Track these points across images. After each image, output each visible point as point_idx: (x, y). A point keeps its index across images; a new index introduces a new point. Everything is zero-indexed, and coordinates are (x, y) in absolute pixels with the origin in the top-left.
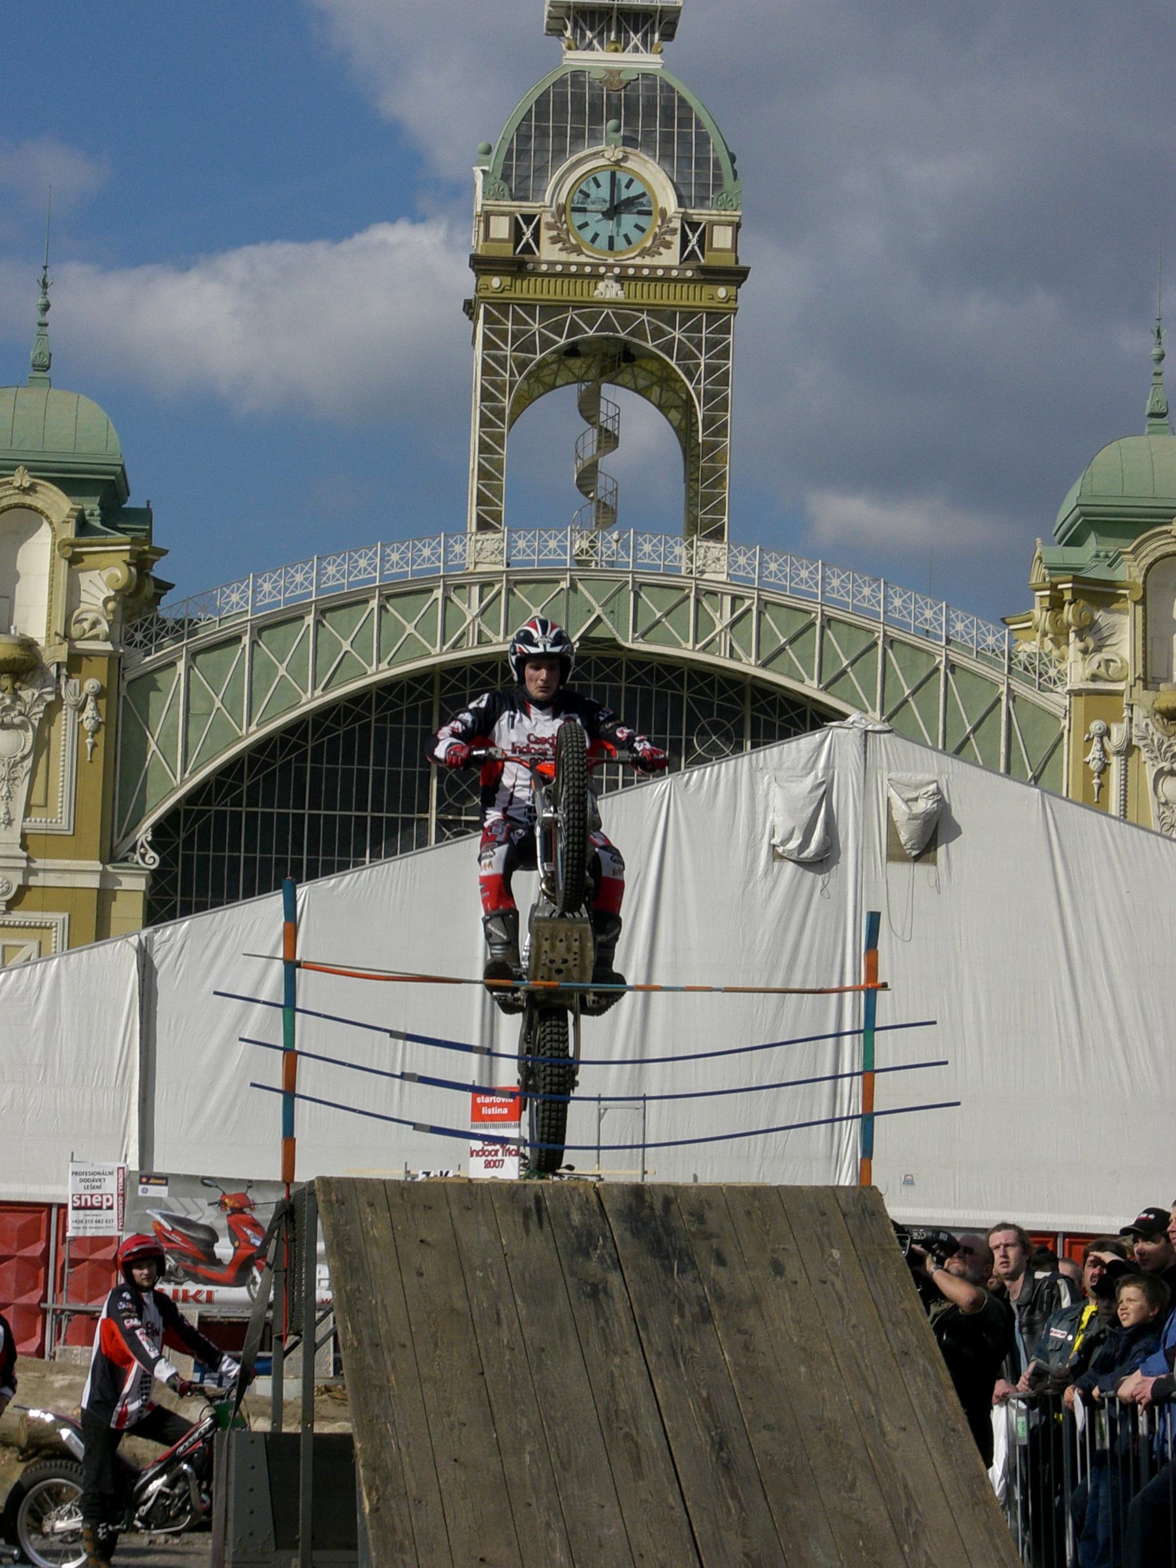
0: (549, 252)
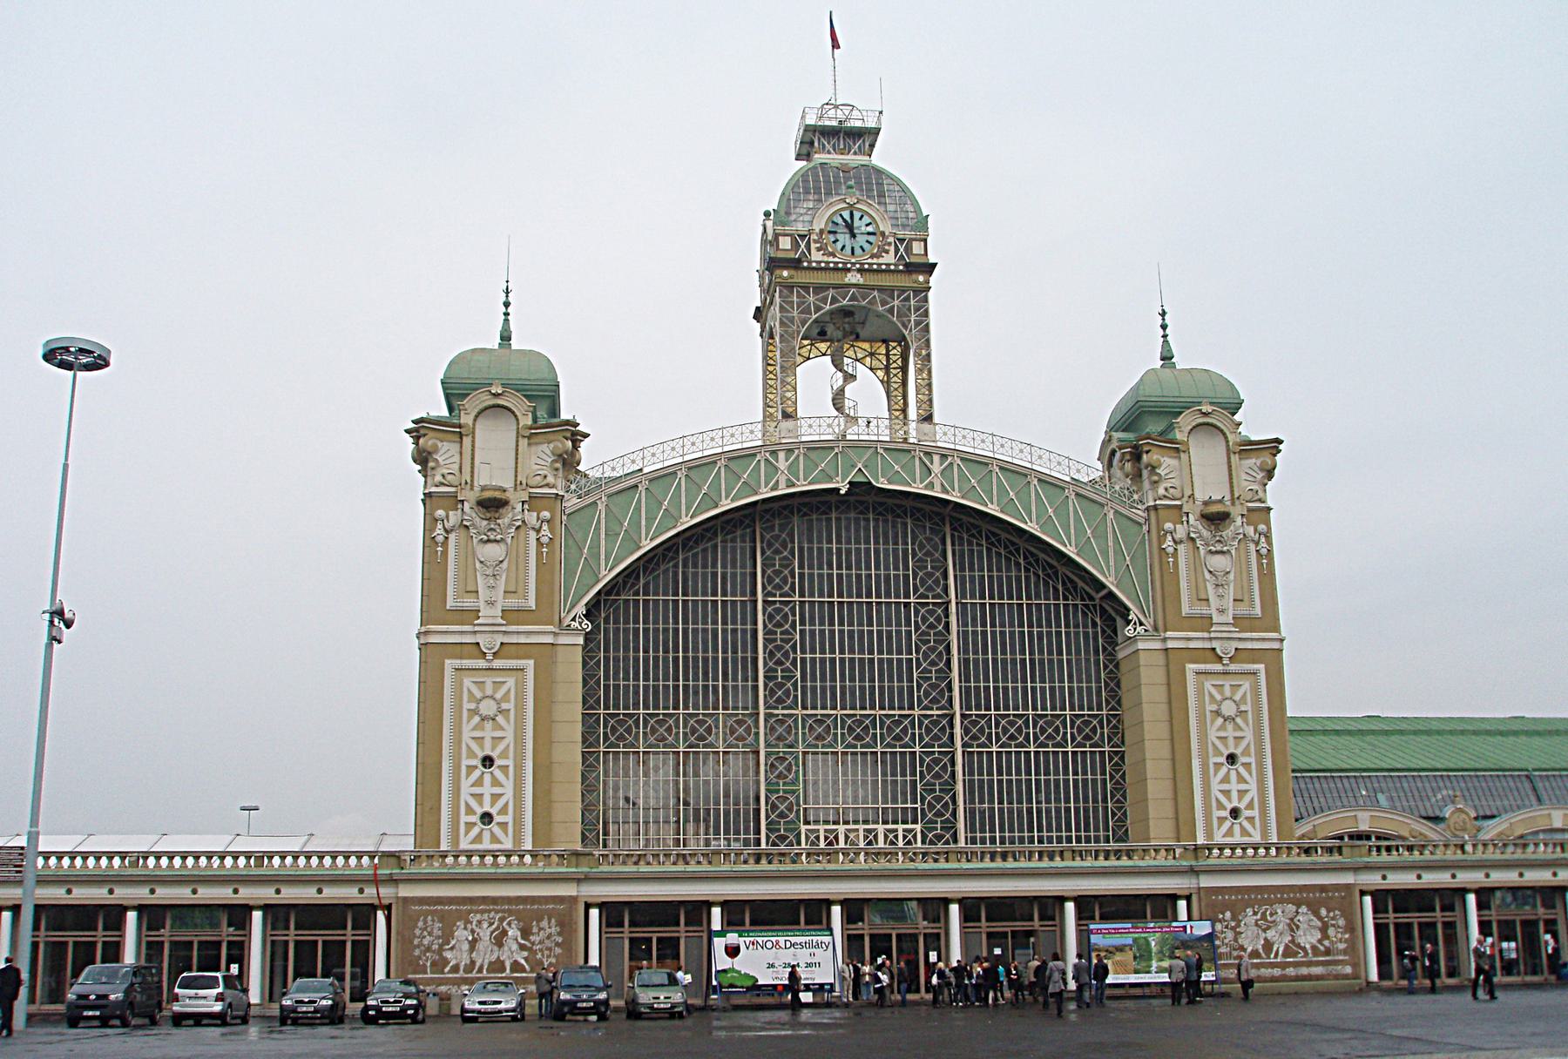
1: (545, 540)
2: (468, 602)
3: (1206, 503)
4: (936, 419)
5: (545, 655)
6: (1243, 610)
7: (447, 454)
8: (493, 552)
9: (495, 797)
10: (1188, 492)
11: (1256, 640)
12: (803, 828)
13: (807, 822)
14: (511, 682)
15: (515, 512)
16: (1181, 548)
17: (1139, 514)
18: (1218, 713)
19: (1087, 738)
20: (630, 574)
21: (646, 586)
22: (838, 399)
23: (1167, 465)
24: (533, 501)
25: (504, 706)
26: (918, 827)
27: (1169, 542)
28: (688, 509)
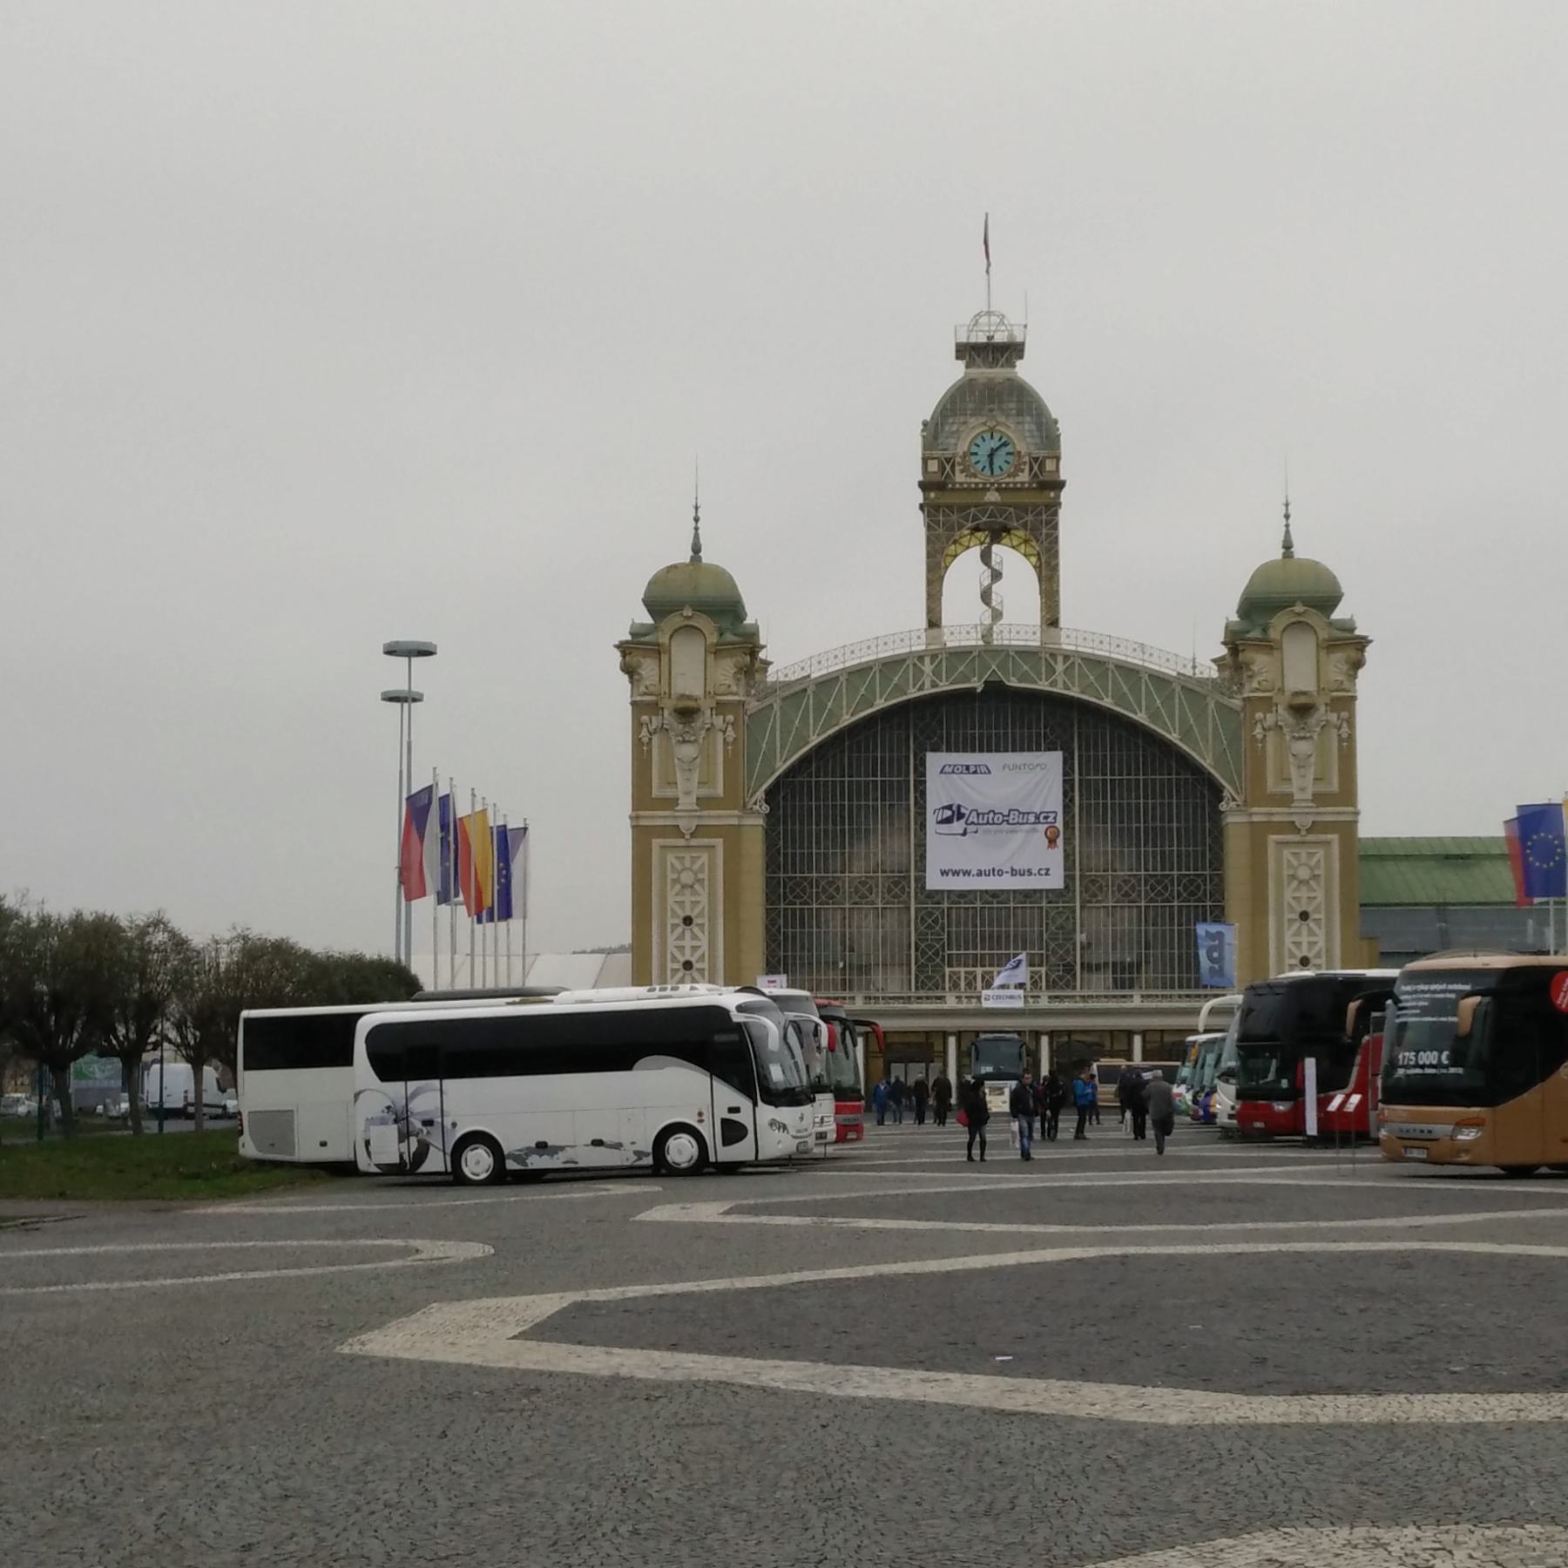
0: (960, 478)
1: (730, 740)
2: (669, 793)
3: (1296, 694)
4: (1062, 624)
5: (731, 835)
6: (1322, 788)
7: (648, 669)
8: (688, 751)
9: (694, 949)
10: (1278, 685)
11: (1330, 814)
12: (947, 970)
13: (950, 965)
14: (705, 857)
15: (706, 718)
16: (1270, 735)
17: (1236, 703)
18: (1293, 877)
19: (1192, 894)
20: (805, 761)
21: (818, 769)
22: (986, 596)
23: (1260, 662)
24: (721, 708)
25: (700, 876)
26: (1043, 970)
27: (1258, 730)
28: (848, 707)
